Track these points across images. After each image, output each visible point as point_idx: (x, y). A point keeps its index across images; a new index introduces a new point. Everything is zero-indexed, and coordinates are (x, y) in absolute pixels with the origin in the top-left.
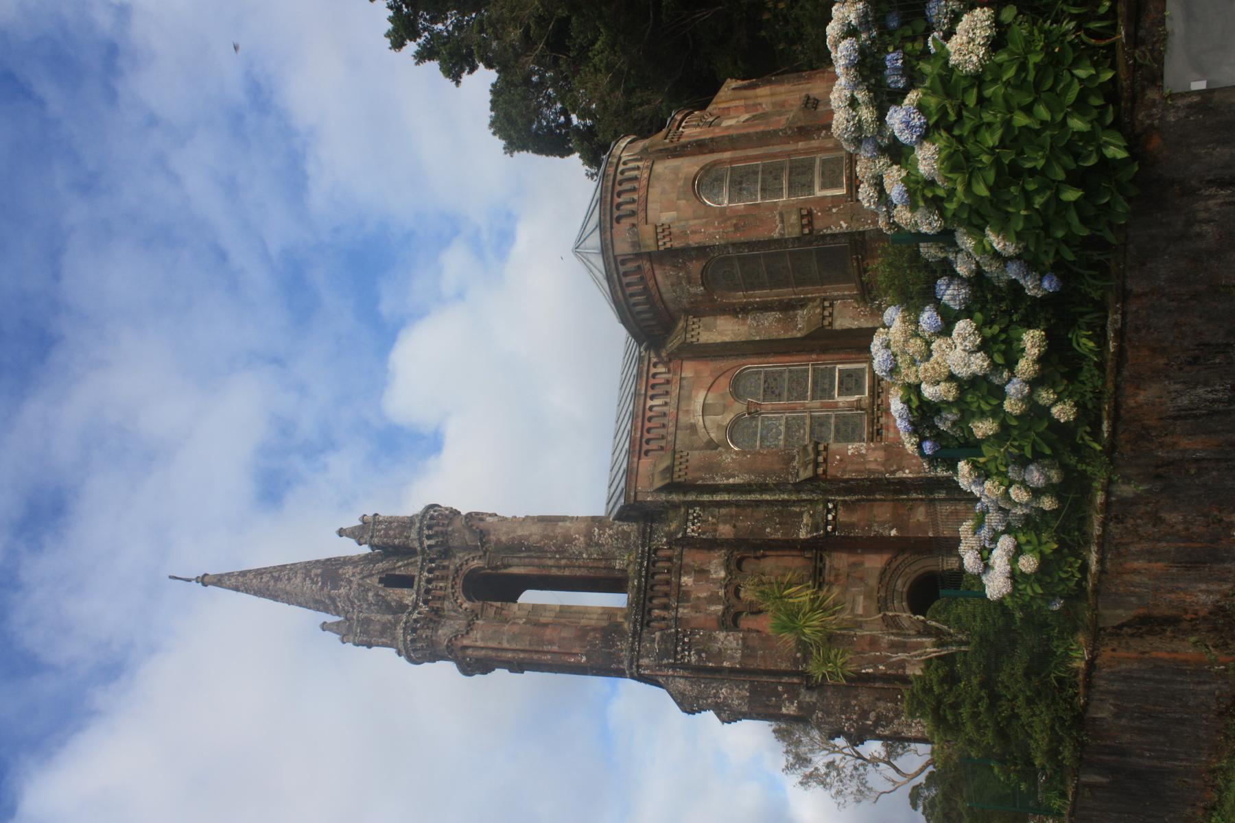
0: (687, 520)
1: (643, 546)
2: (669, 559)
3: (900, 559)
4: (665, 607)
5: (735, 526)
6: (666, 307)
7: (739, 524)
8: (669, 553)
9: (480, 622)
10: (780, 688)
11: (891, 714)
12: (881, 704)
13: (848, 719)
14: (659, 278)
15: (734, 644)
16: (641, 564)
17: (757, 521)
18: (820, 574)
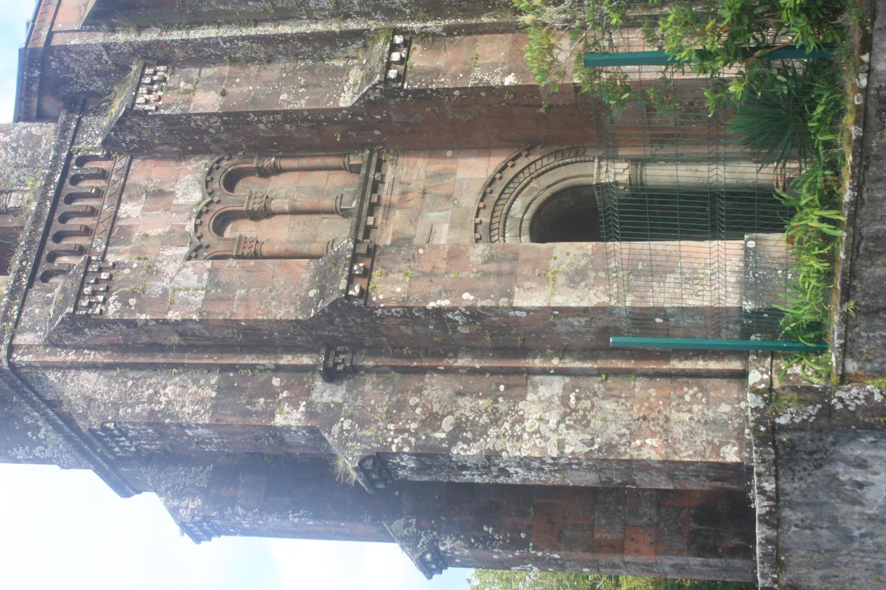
0: (140, 84)
1: (58, 149)
2: (103, 175)
3: (522, 163)
5: (224, 94)
7: (233, 90)
8: (105, 165)
10: (276, 382)
11: (484, 419)
12: (466, 404)
13: (399, 431)
15: (193, 282)
16: (49, 178)
17: (266, 83)
18: (375, 190)
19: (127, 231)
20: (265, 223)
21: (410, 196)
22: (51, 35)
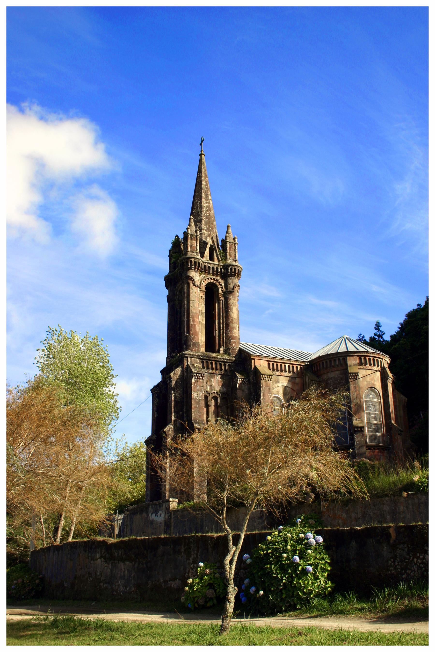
6: (325, 373)
14: (337, 372)
19: (213, 377)
22: (254, 359)
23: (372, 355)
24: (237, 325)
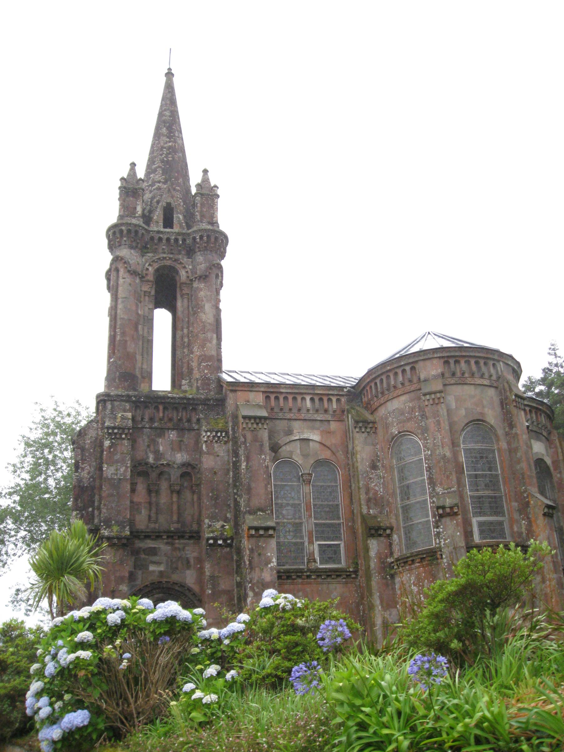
4: (152, 420)
9: (138, 280)
10: (90, 509)
14: (403, 398)
20: (169, 492)
21: (178, 552)
23: (472, 354)
24: (215, 336)
